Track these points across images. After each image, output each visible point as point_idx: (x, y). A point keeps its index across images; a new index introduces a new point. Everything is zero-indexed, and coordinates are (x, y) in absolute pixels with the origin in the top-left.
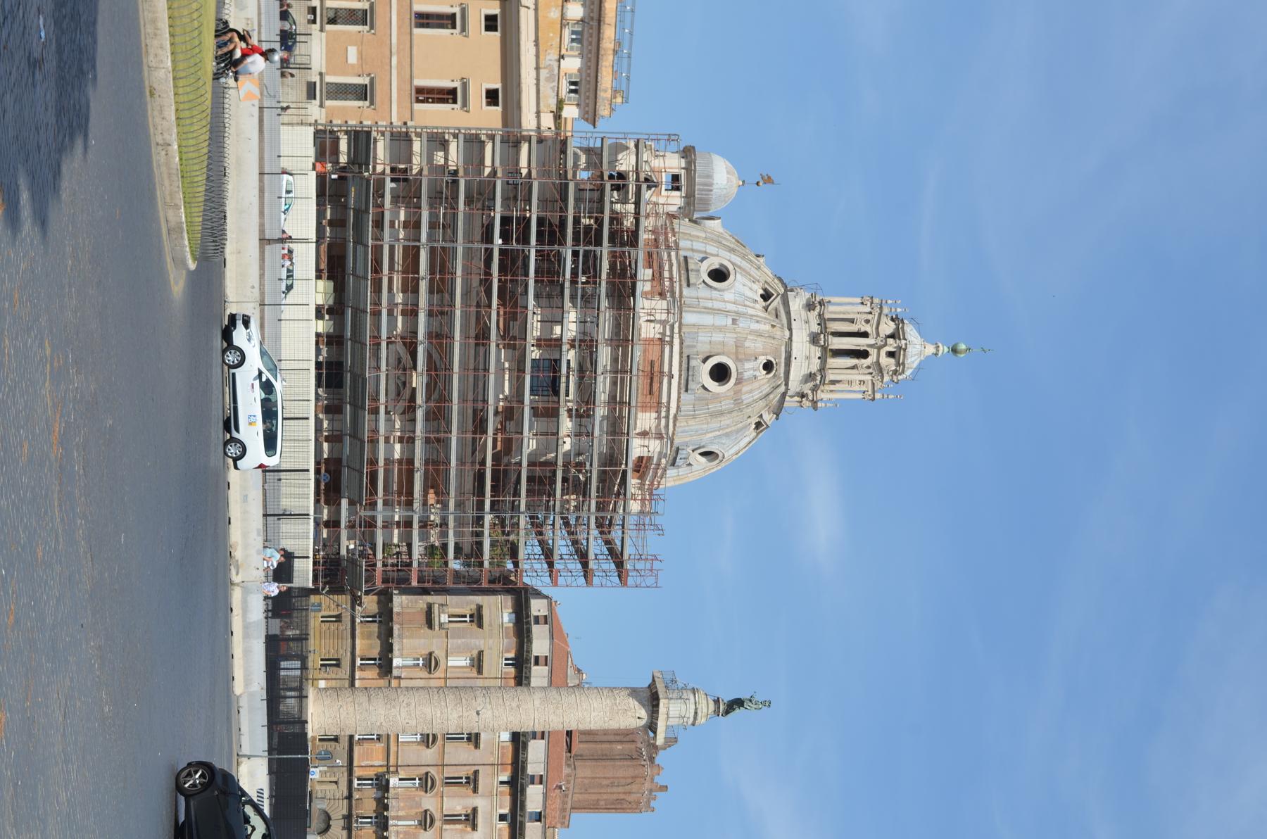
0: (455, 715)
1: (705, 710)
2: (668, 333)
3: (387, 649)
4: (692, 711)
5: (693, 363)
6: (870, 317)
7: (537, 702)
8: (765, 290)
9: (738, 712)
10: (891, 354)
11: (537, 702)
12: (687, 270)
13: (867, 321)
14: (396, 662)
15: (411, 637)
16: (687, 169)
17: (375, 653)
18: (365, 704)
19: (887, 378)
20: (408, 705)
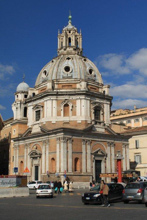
5: (43, 81)
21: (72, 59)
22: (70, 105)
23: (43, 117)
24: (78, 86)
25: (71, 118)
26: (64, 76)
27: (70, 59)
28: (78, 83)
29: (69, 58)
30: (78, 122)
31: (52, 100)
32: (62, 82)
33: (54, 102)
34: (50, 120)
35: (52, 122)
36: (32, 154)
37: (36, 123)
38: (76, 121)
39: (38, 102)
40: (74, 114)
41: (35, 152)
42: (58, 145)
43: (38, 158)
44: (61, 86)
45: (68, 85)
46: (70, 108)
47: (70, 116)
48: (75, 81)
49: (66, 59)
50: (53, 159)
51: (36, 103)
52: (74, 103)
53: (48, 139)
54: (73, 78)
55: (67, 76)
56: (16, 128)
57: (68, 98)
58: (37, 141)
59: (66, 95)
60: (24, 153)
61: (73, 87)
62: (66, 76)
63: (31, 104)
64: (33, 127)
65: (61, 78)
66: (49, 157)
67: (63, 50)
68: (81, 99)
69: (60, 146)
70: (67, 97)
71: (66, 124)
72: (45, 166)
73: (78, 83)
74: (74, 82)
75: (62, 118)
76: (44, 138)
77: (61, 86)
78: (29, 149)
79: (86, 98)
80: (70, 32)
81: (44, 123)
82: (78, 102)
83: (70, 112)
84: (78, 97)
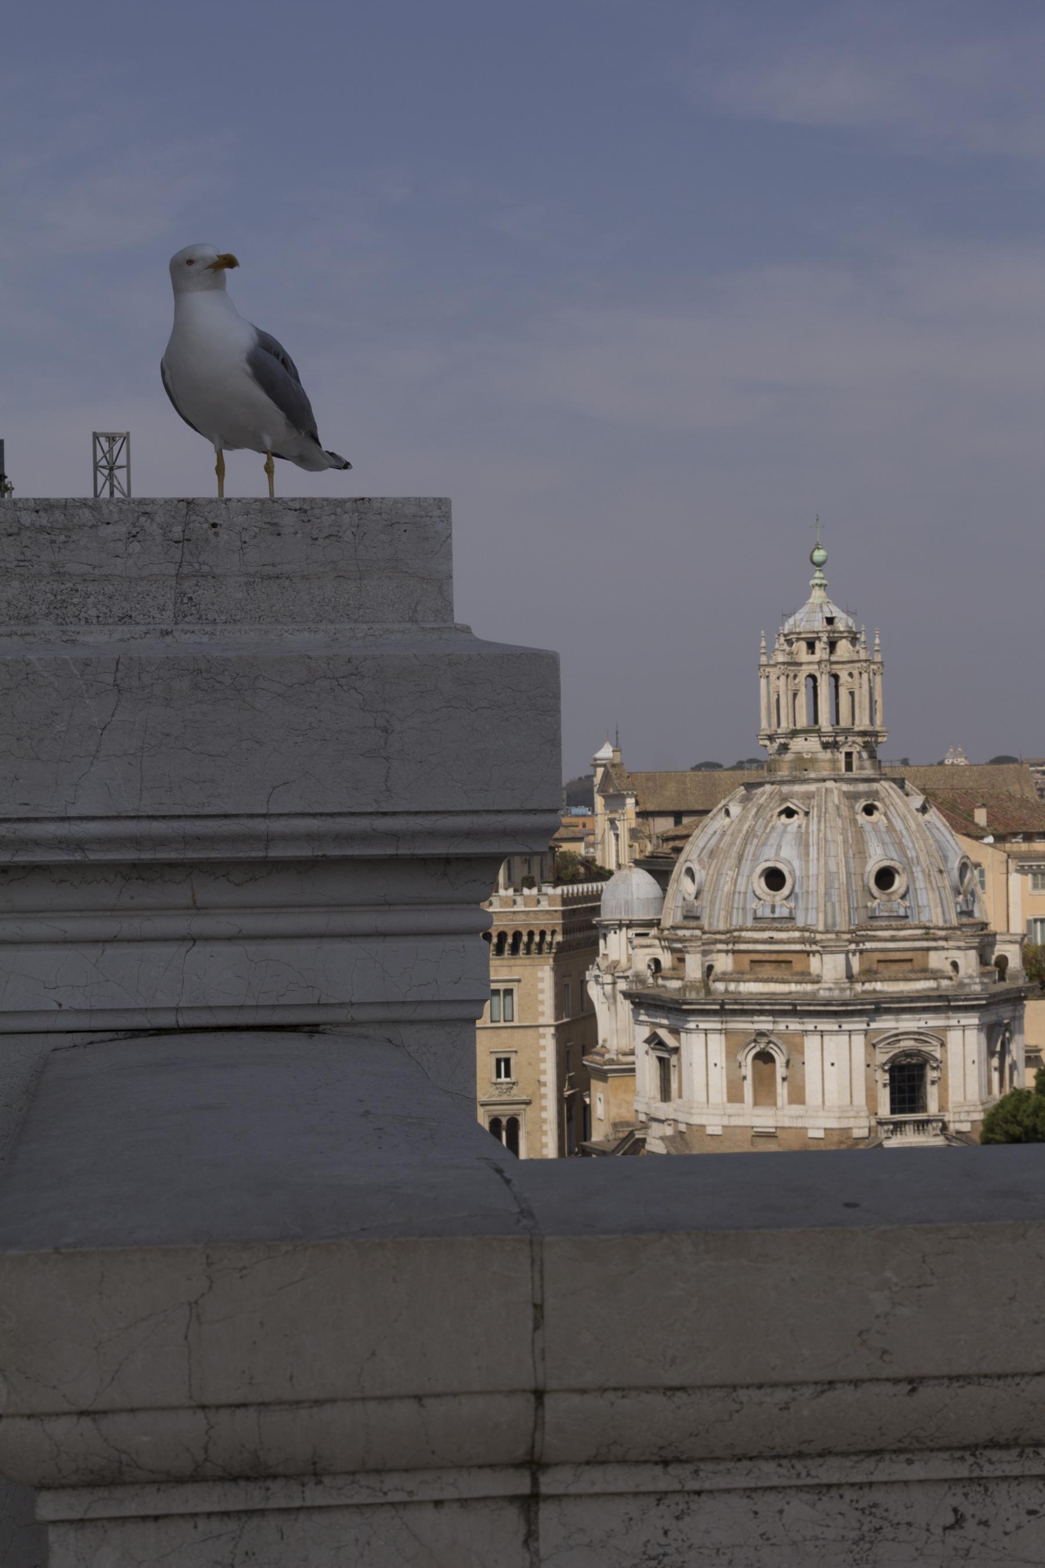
21: (802, 814)
22: (780, 1060)
26: (759, 914)
27: (796, 816)
28: (814, 953)
29: (788, 808)
30: (811, 1134)
31: (706, 1031)
32: (751, 947)
34: (695, 1120)
35: (710, 1130)
38: (801, 1128)
40: (797, 1097)
44: (746, 959)
45: (774, 957)
46: (780, 1071)
47: (779, 1103)
49: (780, 813)
52: (795, 1051)
54: (800, 922)
55: (773, 912)
61: (797, 967)
62: (768, 913)
65: (750, 923)
68: (822, 1033)
70: (764, 1024)
71: (763, 1140)
73: (814, 953)
77: (746, 959)
79: (845, 1027)
80: (811, 646)
82: (811, 1044)
83: (782, 1090)
84: (810, 1024)
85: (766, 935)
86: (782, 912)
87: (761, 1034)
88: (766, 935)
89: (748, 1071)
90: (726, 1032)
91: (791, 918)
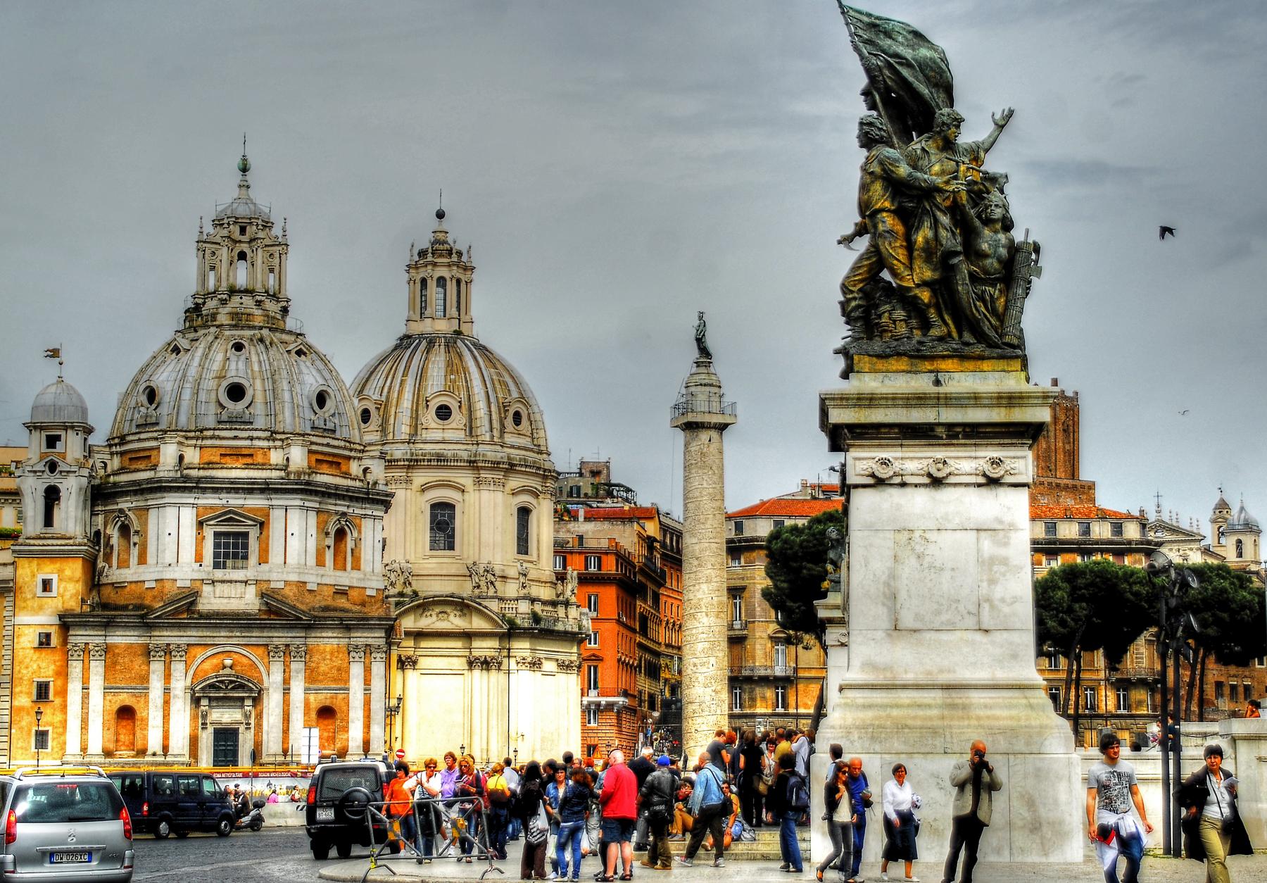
0: (705, 620)
1: (703, 376)
2: (194, 442)
3: (765, 681)
4: (703, 388)
5: (225, 418)
6: (208, 252)
7: (695, 540)
8: (173, 351)
9: (710, 343)
10: (243, 231)
11: (695, 540)
12: (146, 425)
13: (214, 253)
14: (779, 671)
15: (754, 658)
16: (41, 428)
17: (769, 693)
18: (694, 707)
19: (261, 234)
20: (695, 665)
23: (263, 559)
24: (355, 468)
25: (346, 578)
30: (369, 592)
31: (308, 509)
33: (312, 515)
36: (212, 686)
37: (227, 578)
39: (235, 501)
40: (356, 566)
41: (231, 682)
42: (356, 670)
43: (248, 702)
46: (350, 544)
48: (351, 450)
50: (326, 713)
51: (218, 502)
53: (297, 641)
54: (338, 435)
56: (60, 571)
57: (345, 509)
58: (235, 641)
59: (343, 497)
60: (145, 679)
61: (344, 468)
63: (192, 501)
64: (207, 589)
66: (307, 704)
67: (248, 301)
69: (368, 671)
72: (286, 731)
74: (347, 453)
75: (332, 576)
76: (280, 638)
78: (178, 668)
81: (281, 585)
85: (325, 441)
86: (330, 426)
87: (344, 514)
88: (325, 441)
89: (330, 541)
90: (318, 512)
91: (334, 431)
